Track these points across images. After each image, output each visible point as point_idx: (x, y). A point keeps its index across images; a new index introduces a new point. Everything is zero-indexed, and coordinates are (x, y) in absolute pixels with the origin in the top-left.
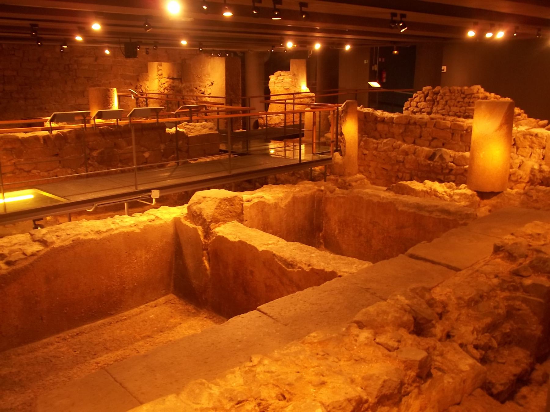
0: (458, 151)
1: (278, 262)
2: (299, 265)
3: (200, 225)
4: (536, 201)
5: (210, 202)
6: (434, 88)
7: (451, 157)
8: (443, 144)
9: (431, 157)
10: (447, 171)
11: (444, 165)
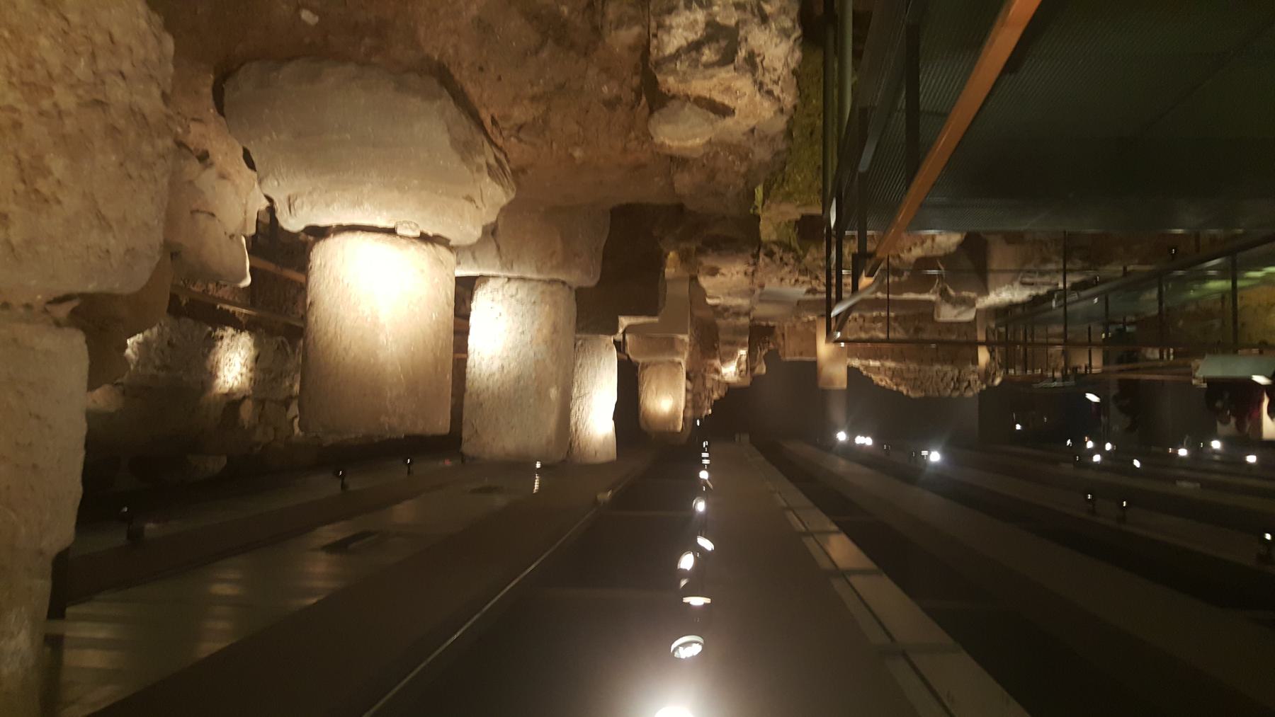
6: (961, 395)
9: (917, 330)
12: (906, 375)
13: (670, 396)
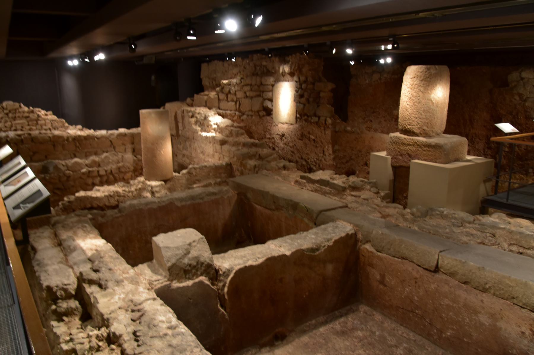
0: (65, 159)
1: (307, 253)
2: (323, 245)
3: (202, 275)
4: (196, 176)
5: (198, 245)
7: (63, 165)
8: (46, 157)
10: (65, 178)
11: (61, 175)
12: (24, 121)
13: (434, 102)
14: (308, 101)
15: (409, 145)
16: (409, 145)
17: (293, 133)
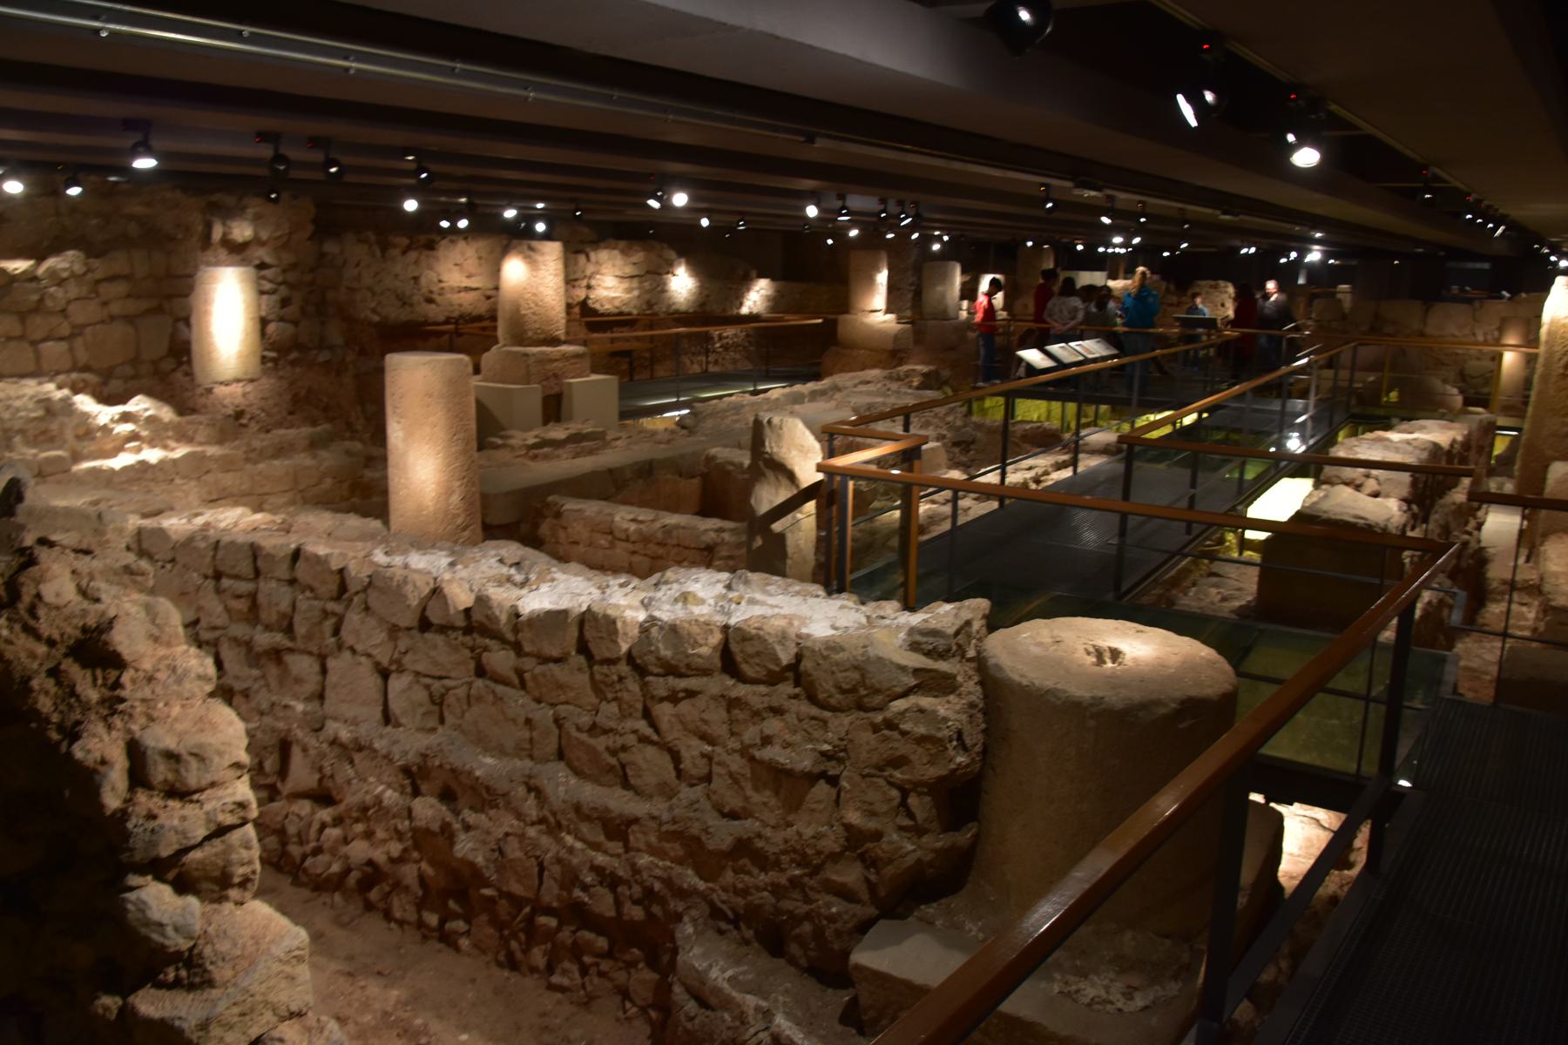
14: (303, 311)
15: (557, 360)
16: (557, 360)
17: (271, 402)
